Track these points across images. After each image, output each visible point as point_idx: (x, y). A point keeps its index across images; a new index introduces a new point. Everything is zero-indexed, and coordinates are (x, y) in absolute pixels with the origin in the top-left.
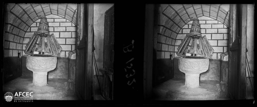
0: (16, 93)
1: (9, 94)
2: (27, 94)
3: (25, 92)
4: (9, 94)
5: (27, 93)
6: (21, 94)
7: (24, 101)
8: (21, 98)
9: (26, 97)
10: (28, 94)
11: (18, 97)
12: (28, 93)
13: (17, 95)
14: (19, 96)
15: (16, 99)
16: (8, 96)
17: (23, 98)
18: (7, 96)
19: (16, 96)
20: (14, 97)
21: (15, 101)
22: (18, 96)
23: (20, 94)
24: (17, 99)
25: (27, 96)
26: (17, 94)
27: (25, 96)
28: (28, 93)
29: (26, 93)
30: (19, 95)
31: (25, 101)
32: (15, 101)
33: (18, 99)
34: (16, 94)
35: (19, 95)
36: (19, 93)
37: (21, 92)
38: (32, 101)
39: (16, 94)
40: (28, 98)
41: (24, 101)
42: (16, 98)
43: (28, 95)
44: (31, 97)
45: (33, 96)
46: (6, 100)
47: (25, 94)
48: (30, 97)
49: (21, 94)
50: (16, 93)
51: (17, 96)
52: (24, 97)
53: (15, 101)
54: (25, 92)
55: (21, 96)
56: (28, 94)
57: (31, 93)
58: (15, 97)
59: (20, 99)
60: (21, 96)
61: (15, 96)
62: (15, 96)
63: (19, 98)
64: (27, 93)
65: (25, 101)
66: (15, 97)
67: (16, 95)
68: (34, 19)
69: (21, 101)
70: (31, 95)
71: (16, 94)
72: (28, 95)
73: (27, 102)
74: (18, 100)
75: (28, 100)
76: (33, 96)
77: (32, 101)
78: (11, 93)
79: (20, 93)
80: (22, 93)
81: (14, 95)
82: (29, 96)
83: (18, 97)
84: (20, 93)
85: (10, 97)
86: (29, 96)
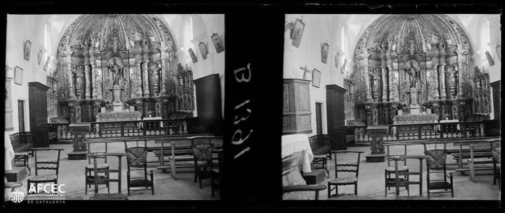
6: (41, 188)
7: (47, 202)
8: (41, 195)
9: (51, 193)
17: (46, 195)
24: (33, 197)
29: (51, 186)
31: (49, 202)
33: (36, 197)
38: (64, 202)
41: (47, 202)
44: (61, 194)
45: (64, 192)
49: (41, 188)
52: (47, 194)
54: (49, 185)
58: (29, 194)
63: (38, 197)
65: (49, 202)
70: (61, 190)
74: (36, 201)
75: (55, 201)
77: (64, 202)
80: (43, 187)
84: (40, 186)
85: (20, 193)
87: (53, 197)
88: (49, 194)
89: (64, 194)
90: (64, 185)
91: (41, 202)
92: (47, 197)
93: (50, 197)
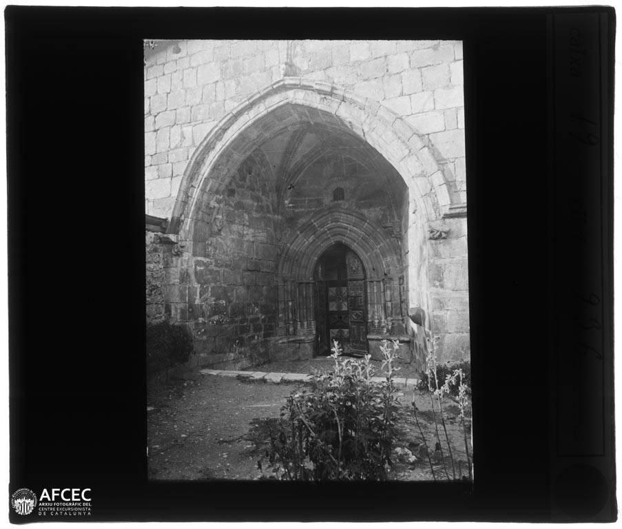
0: (45, 491)
1: (25, 495)
2: (74, 495)
3: (69, 490)
4: (25, 495)
5: (73, 490)
6: (58, 495)
7: (66, 513)
8: (58, 504)
9: (71, 501)
10: (78, 495)
11: (49, 502)
12: (76, 492)
13: (48, 496)
14: (53, 499)
15: (43, 507)
16: (23, 500)
17: (64, 504)
18: (19, 501)
19: (45, 500)
20: (39, 502)
22: (49, 499)
23: (54, 495)
25: (73, 499)
26: (47, 493)
27: (69, 500)
28: (76, 492)
29: (71, 492)
30: (51, 498)
33: (50, 507)
34: (45, 495)
35: (51, 498)
36: (54, 490)
37: (59, 490)
38: (89, 513)
39: (45, 495)
40: (77, 506)
41: (66, 513)
43: (76, 497)
44: (86, 502)
45: (90, 500)
46: (17, 511)
47: (68, 495)
48: (82, 501)
49: (58, 495)
50: (45, 491)
51: (47, 499)
52: (66, 502)
53: (43, 513)
54: (69, 490)
55: (58, 499)
56: (78, 495)
58: (41, 502)
59: (56, 506)
60: (58, 499)
61: (41, 499)
62: (41, 499)
63: (53, 507)
66: (41, 502)
67: (43, 496)
68: (183, 216)
69: (58, 512)
70: (86, 497)
72: (76, 497)
76: (90, 500)
77: (89, 513)
78: (31, 492)
79: (56, 492)
80: (60, 492)
81: (39, 497)
82: (79, 500)
83: (49, 502)
84: (56, 492)
85: (27, 501)
86: (79, 500)
87: (74, 507)
88: (69, 502)
89: (88, 502)
90: (89, 490)
91: (57, 513)
92: (66, 507)
93: (70, 507)
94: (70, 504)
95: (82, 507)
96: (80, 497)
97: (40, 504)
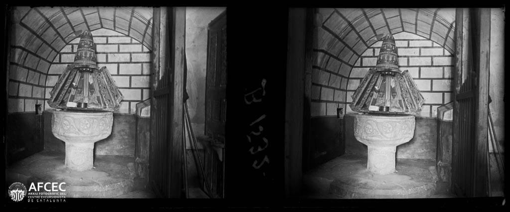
0: (33, 184)
1: (18, 187)
2: (53, 187)
3: (50, 183)
4: (18, 187)
5: (53, 183)
6: (42, 187)
7: (48, 200)
8: (42, 194)
9: (51, 192)
10: (56, 187)
11: (36, 192)
12: (55, 185)
13: (34, 188)
14: (39, 190)
15: (31, 195)
16: (16, 191)
17: (46, 194)
18: (14, 191)
19: (33, 191)
20: (28, 192)
21: (31, 199)
22: (36, 190)
23: (39, 187)
24: (33, 195)
25: (53, 190)
26: (34, 186)
27: (50, 191)
28: (55, 185)
29: (51, 185)
30: (37, 189)
31: (49, 200)
32: (31, 199)
33: (36, 195)
34: (33, 187)
35: (37, 189)
36: (39, 184)
37: (42, 183)
38: (64, 200)
39: (33, 187)
40: (56, 195)
41: (48, 200)
42: (31, 194)
43: (55, 189)
44: (62, 192)
45: (65, 190)
47: (49, 187)
48: (60, 191)
49: (42, 187)
50: (33, 184)
51: (34, 190)
52: (48, 192)
53: (31, 200)
54: (50, 183)
55: (42, 190)
56: (56, 187)
57: (62, 185)
58: (30, 192)
59: (41, 195)
60: (42, 190)
61: (30, 190)
62: (30, 190)
63: (38, 195)
64: (53, 183)
65: (49, 200)
66: (30, 192)
67: (31, 188)
68: (369, 42)
69: (42, 199)
70: (61, 188)
71: (31, 186)
72: (55, 189)
73: (54, 201)
74: (36, 199)
75: (56, 199)
76: (65, 190)
77: (64, 200)
78: (23, 185)
79: (40, 185)
80: (43, 185)
81: (28, 189)
82: (57, 190)
83: (36, 192)
84: (40, 185)
85: (20, 191)
86: (57, 190)
92: (48, 195)
93: (51, 195)
94: (51, 194)
95: (60, 195)
96: (58, 188)
97: (29, 194)
